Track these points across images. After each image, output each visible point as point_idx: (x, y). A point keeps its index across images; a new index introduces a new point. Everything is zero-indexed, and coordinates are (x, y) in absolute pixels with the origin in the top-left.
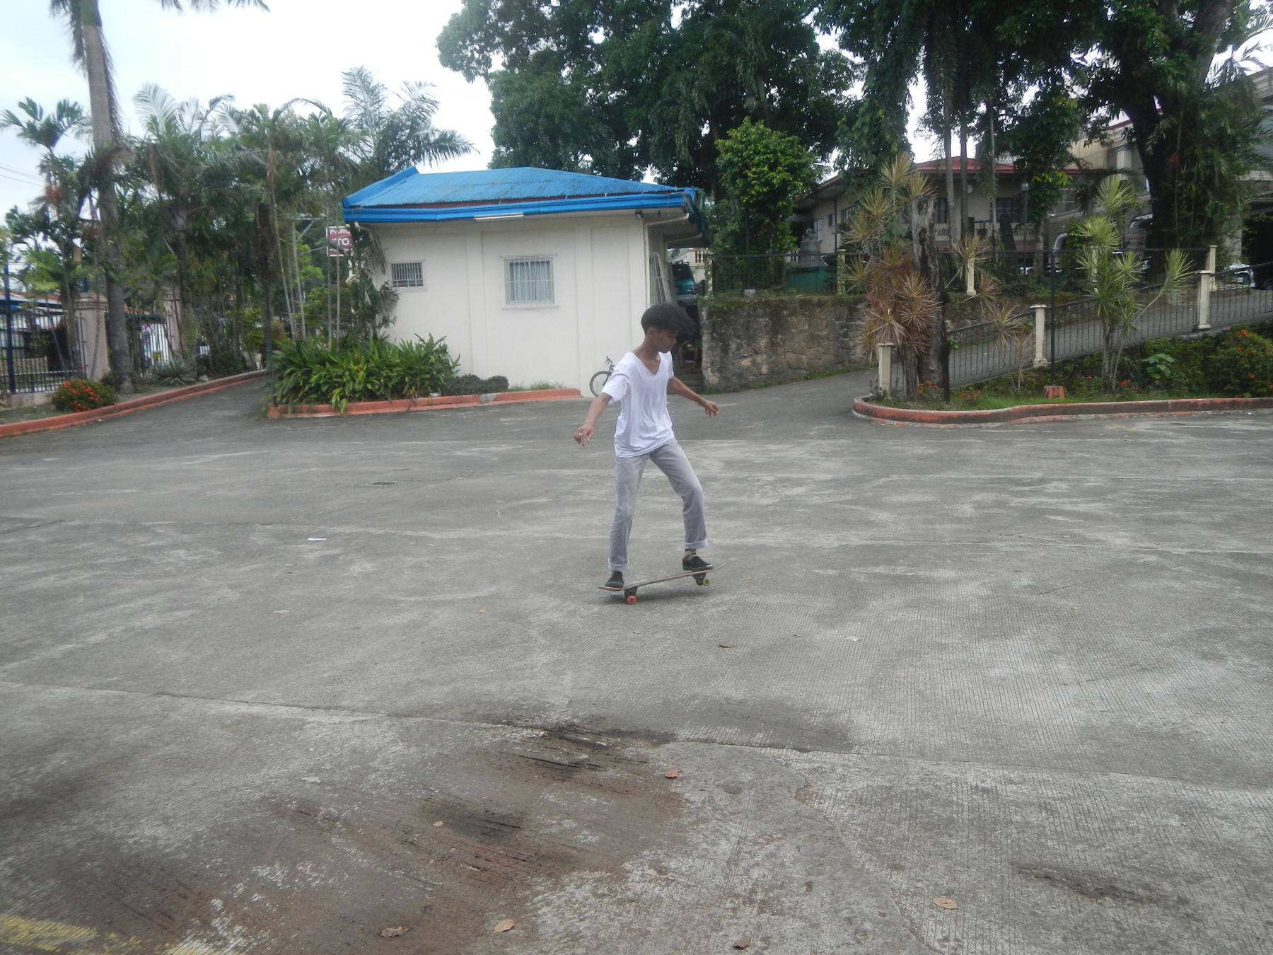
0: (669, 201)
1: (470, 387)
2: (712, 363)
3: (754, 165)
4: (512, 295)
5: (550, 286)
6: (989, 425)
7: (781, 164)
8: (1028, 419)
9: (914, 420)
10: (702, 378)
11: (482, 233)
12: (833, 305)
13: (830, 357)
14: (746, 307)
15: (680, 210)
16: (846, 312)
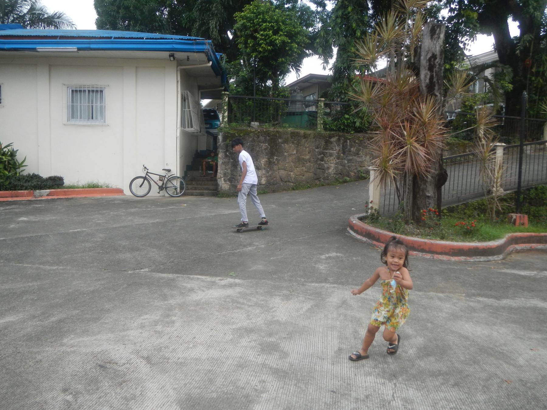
0: (195, 47)
1: (26, 184)
2: (225, 174)
3: (261, 30)
4: (73, 114)
5: (102, 110)
6: (495, 258)
7: (282, 30)
8: (511, 248)
9: (423, 251)
10: (217, 185)
11: (50, 66)
12: (314, 138)
13: (311, 175)
14: (251, 135)
15: (203, 56)
16: (323, 143)
